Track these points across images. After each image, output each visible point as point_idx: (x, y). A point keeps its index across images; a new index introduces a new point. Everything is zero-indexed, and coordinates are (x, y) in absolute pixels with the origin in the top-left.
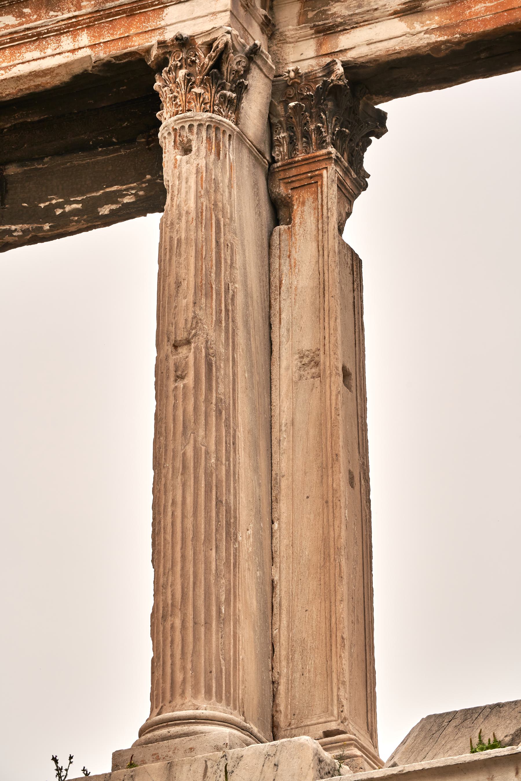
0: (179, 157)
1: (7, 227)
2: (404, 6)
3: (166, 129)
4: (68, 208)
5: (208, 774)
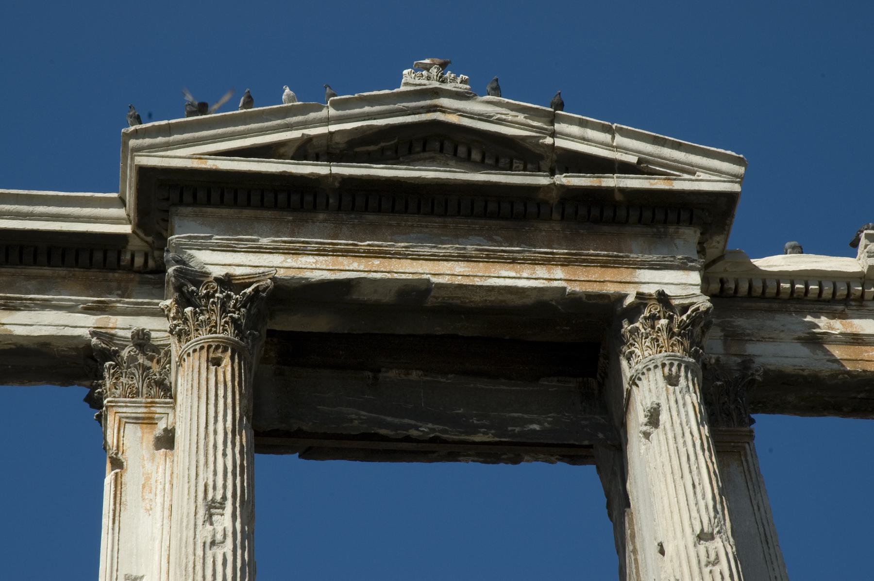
2: (808, 335)
3: (652, 361)
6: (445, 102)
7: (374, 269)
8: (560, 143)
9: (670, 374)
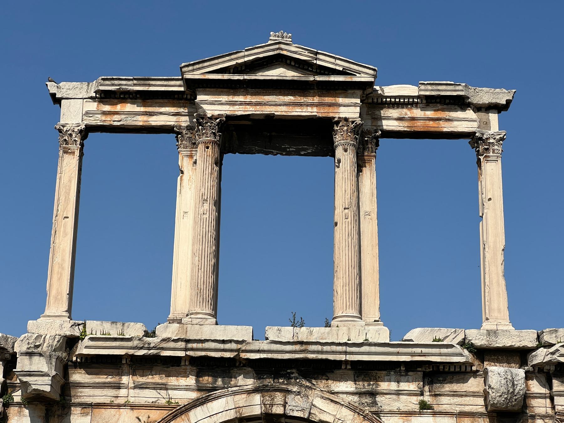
0: (344, 153)
1: (272, 150)
4: (291, 149)
5: (360, 333)
6: (283, 46)
7: (257, 110)
8: (319, 63)
9: (345, 148)
